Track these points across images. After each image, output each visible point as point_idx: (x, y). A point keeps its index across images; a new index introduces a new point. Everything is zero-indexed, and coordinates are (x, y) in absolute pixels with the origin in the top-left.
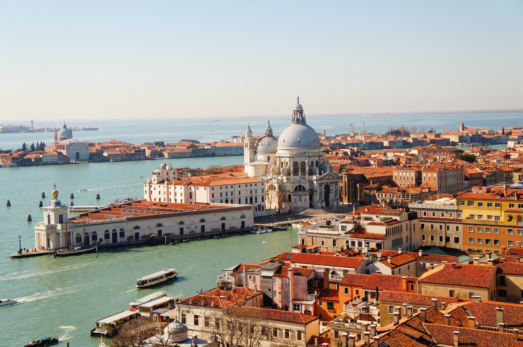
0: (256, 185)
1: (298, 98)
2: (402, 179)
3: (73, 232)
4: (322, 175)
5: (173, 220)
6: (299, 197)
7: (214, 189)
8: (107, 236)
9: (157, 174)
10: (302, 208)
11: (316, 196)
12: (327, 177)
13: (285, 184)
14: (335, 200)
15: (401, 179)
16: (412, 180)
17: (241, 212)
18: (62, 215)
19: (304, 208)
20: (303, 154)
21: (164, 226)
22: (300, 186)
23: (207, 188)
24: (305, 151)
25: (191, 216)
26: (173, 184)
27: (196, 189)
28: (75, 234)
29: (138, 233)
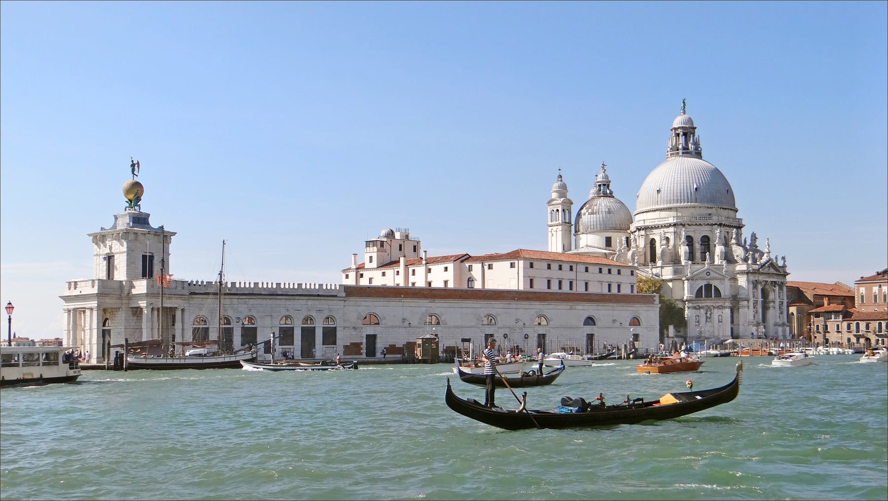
0: (619, 272)
2: (880, 299)
3: (183, 310)
4: (758, 263)
6: (706, 313)
8: (286, 335)
11: (746, 309)
12: (766, 270)
13: (670, 284)
14: (780, 325)
15: (876, 300)
17: (631, 308)
18: (152, 258)
19: (719, 339)
21: (446, 324)
22: (708, 287)
23: (516, 262)
24: (710, 211)
25: (514, 304)
26: (424, 262)
27: (486, 267)
28: (189, 318)
29: (374, 336)
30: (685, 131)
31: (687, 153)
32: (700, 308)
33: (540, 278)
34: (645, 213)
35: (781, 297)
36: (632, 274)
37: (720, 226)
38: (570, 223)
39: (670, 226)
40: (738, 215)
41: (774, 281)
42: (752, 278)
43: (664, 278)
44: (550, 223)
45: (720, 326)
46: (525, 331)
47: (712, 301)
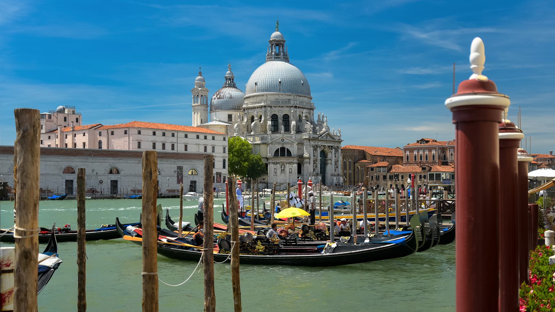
0: (213, 138)
1: (278, 23)
4: (318, 133)
5: (52, 163)
6: (281, 167)
7: (142, 133)
9: (47, 117)
10: (285, 185)
11: (308, 164)
14: (335, 176)
15: (415, 160)
16: (434, 159)
17: (189, 163)
20: (287, 104)
22: (283, 149)
24: (289, 97)
27: (110, 133)
30: (277, 43)
31: (279, 58)
32: (277, 163)
33: (147, 141)
34: (248, 99)
35: (337, 156)
36: (224, 139)
37: (296, 108)
38: (207, 105)
39: (262, 107)
40: (312, 101)
41: (331, 146)
42: (312, 143)
43: (255, 143)
44: (193, 105)
45: (290, 176)
46: (100, 178)
47: (285, 159)
